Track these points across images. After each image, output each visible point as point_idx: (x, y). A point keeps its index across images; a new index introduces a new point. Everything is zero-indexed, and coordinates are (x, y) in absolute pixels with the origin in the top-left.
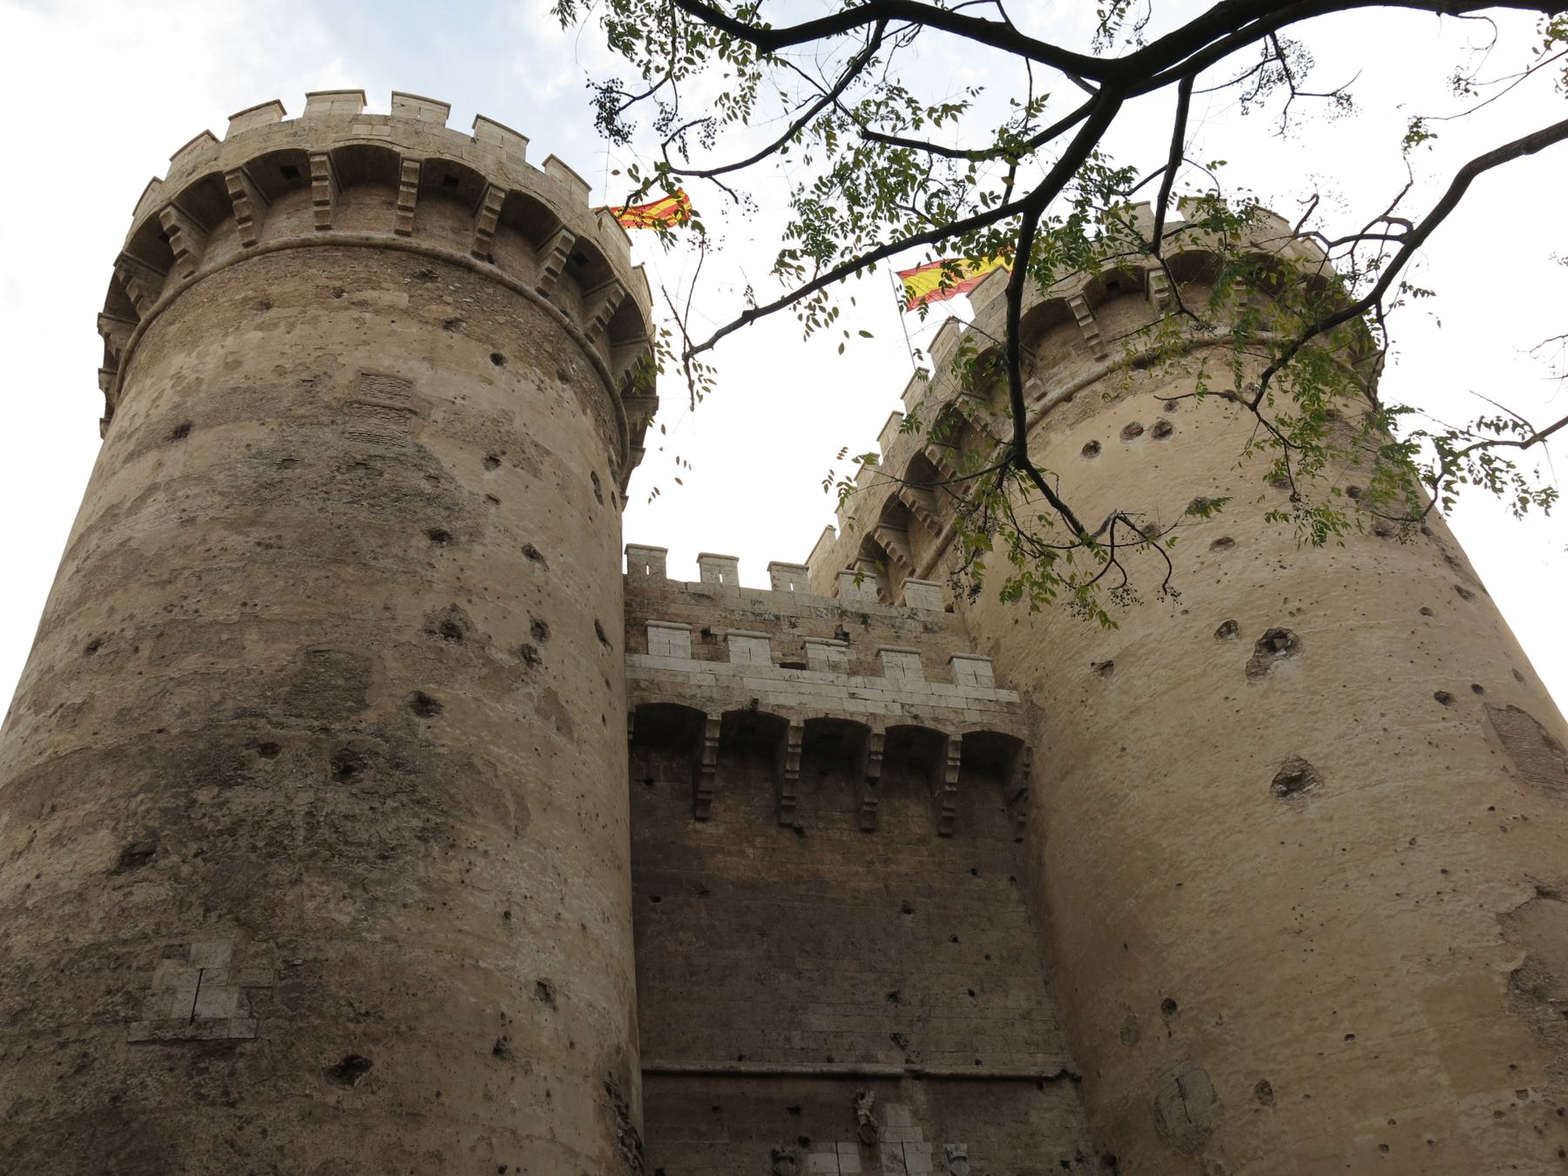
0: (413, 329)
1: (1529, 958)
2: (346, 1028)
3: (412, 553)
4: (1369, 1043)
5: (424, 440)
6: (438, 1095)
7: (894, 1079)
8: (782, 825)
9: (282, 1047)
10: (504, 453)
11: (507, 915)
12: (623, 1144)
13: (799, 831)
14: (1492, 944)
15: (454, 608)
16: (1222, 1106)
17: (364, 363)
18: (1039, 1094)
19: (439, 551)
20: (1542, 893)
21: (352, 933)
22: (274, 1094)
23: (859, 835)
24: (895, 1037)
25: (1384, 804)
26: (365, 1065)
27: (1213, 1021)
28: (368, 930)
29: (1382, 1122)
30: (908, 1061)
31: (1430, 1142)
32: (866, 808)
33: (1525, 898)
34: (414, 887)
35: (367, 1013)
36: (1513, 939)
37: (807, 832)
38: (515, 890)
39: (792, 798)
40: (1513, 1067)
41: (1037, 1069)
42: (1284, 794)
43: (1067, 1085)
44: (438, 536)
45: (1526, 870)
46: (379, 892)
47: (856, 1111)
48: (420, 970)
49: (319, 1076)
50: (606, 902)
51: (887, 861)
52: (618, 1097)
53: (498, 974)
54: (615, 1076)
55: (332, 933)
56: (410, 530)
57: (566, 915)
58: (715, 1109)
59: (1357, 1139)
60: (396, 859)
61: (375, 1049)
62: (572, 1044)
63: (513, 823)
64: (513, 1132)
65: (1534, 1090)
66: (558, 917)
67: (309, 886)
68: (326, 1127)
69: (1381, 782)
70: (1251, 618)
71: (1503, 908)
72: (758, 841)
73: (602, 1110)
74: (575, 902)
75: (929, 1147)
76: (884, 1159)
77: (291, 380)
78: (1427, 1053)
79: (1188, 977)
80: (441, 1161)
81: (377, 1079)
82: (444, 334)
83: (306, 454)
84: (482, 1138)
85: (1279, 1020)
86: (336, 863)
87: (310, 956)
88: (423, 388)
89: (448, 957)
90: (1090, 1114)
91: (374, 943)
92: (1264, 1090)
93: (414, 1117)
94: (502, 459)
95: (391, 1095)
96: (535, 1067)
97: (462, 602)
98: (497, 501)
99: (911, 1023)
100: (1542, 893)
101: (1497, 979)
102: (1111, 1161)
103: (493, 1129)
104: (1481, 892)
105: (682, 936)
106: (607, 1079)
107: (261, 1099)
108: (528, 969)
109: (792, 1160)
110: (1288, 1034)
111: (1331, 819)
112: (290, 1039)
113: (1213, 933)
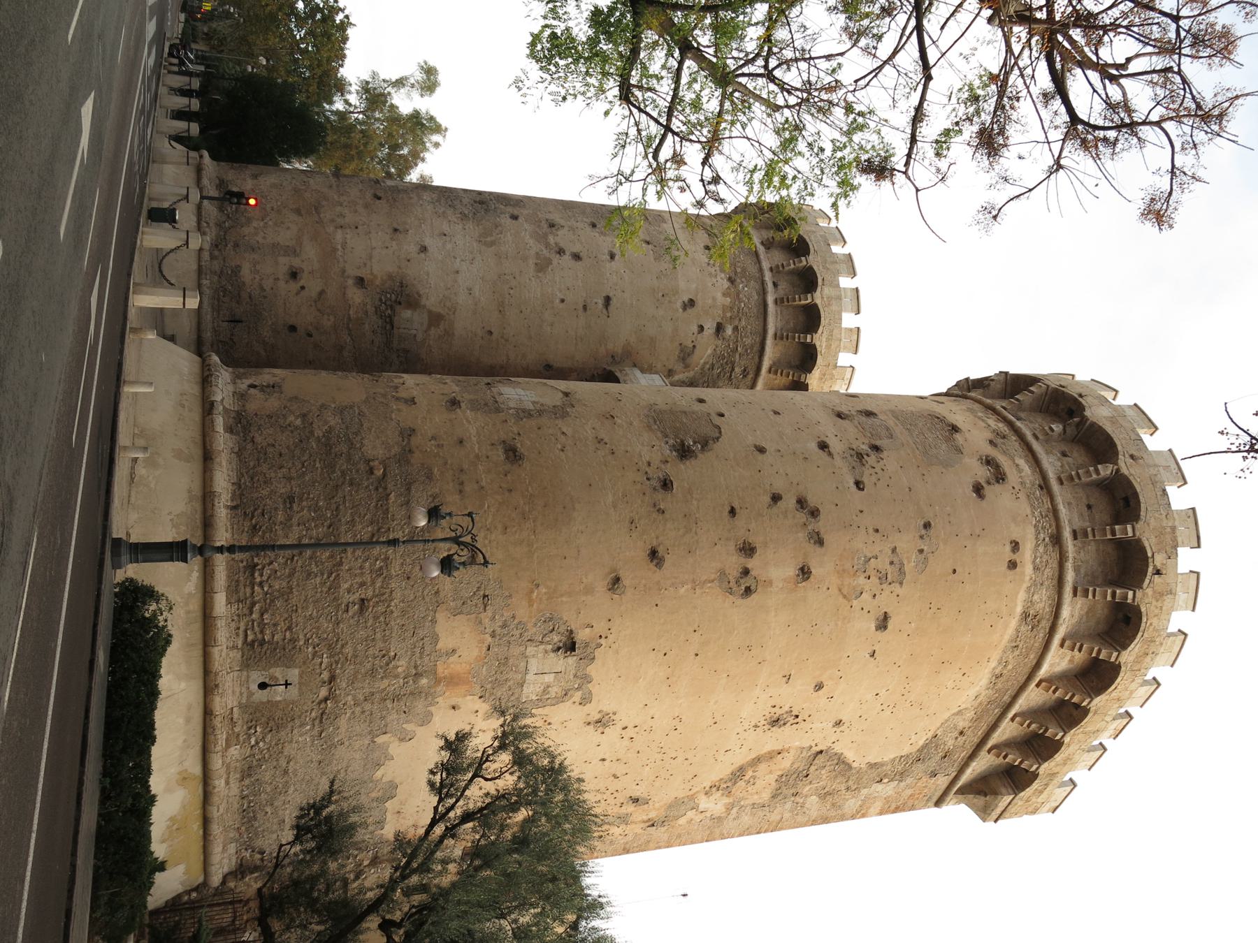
73: (390, 277)
108: (428, 242)
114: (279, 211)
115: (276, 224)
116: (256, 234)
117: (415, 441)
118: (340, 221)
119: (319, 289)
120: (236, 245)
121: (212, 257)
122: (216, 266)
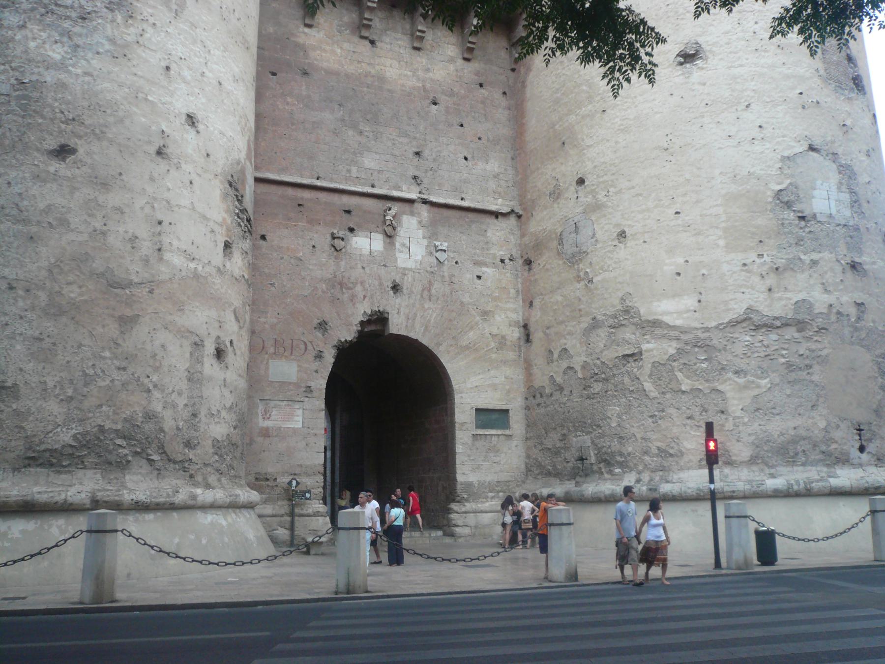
1: (791, 184)
2: (59, 127)
4: (687, 218)
6: (120, 174)
7: (411, 201)
8: (362, 37)
9: (19, 134)
11: (168, 68)
12: (238, 217)
13: (372, 42)
14: (773, 173)
16: (596, 241)
18: (495, 221)
20: (812, 148)
21: (61, 66)
22: (14, 161)
23: (413, 52)
24: (415, 178)
25: (739, 80)
26: (73, 151)
27: (604, 193)
28: (73, 66)
29: (681, 260)
30: (420, 193)
31: (703, 275)
32: (418, 33)
34: (104, 41)
35: (74, 119)
36: (785, 172)
37: (378, 44)
38: (174, 53)
39: (370, 20)
40: (761, 241)
41: (497, 207)
42: (681, 64)
43: (513, 220)
45: (806, 133)
46: (80, 41)
47: (385, 216)
48: (109, 97)
49: (43, 154)
50: (236, 70)
51: (428, 70)
52: (237, 190)
53: (160, 105)
54: (235, 178)
55: (49, 65)
57: (207, 73)
58: (299, 205)
59: (665, 268)
60: (91, 20)
61: (79, 142)
62: (208, 155)
63: (174, 7)
64: (168, 202)
65: (768, 255)
66: (203, 74)
67: (31, 31)
68: (48, 185)
69: (741, 66)
71: (786, 154)
72: (346, 45)
73: (225, 196)
74: (215, 66)
75: (425, 242)
76: (398, 245)
78: (717, 228)
79: (595, 167)
80: (122, 213)
81: (81, 161)
84: (148, 203)
85: (641, 198)
86: (49, 19)
87: (34, 78)
89: (127, 90)
90: (523, 236)
91: (77, 75)
92: (622, 235)
93: (105, 186)
95: (90, 171)
96: (183, 166)
99: (426, 171)
100: (812, 148)
101: (769, 193)
102: (528, 263)
103: (155, 199)
104: (778, 143)
105: (289, 100)
106: (229, 178)
107: (6, 163)
108: (181, 104)
109: (343, 239)
110: (644, 207)
111: (704, 84)
112: (24, 129)
113: (616, 142)
114: (129, 358)
115: (157, 369)
116: (174, 406)
118: (146, 248)
119: (233, 318)
120: (188, 444)
121: (208, 486)
122: (213, 479)
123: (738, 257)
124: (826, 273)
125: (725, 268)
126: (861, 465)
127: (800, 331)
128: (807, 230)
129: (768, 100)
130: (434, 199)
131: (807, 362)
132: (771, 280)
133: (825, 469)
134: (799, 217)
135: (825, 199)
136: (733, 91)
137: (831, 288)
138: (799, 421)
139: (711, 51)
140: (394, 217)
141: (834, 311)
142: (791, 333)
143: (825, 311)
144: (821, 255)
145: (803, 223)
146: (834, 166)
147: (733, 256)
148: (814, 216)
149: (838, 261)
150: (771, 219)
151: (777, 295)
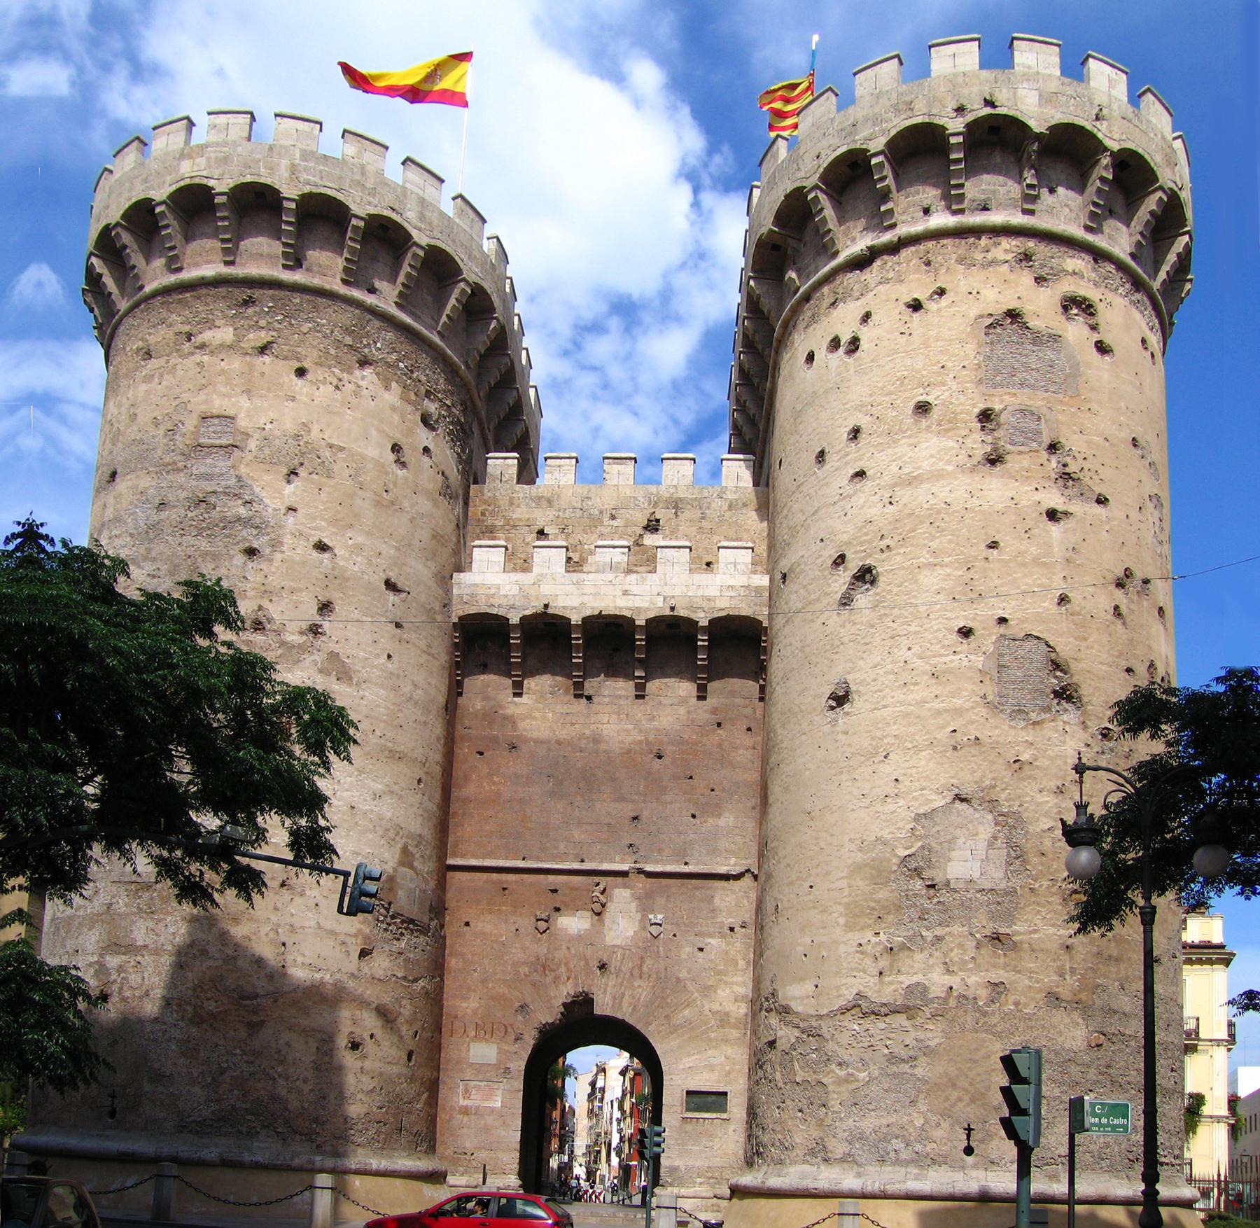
0: (236, 364)
3: (233, 571)
5: (243, 470)
7: (624, 874)
10: (302, 464)
15: (260, 608)
17: (203, 408)
19: (250, 565)
25: (880, 725)
33: (943, 803)
44: (251, 552)
45: (954, 781)
56: (231, 552)
69: (885, 707)
70: (856, 552)
71: (921, 811)
77: (161, 432)
82: (259, 360)
83: (171, 497)
88: (242, 423)
94: (300, 471)
97: (265, 603)
98: (295, 510)
117: (1065, 993)
123: (855, 937)
124: (952, 950)
125: (842, 949)
126: (963, 1168)
127: (908, 1019)
128: (936, 900)
129: (910, 746)
130: (649, 868)
131: (911, 1053)
132: (884, 963)
133: (916, 1171)
134: (928, 886)
135: (969, 860)
136: (873, 739)
137: (955, 969)
138: (893, 1119)
139: (858, 692)
140: (603, 892)
141: (955, 994)
142: (901, 1020)
143: (943, 995)
144: (947, 929)
145: (932, 892)
146: (990, 817)
147: (850, 935)
148: (948, 883)
149: (972, 935)
150: (892, 891)
151: (887, 979)
